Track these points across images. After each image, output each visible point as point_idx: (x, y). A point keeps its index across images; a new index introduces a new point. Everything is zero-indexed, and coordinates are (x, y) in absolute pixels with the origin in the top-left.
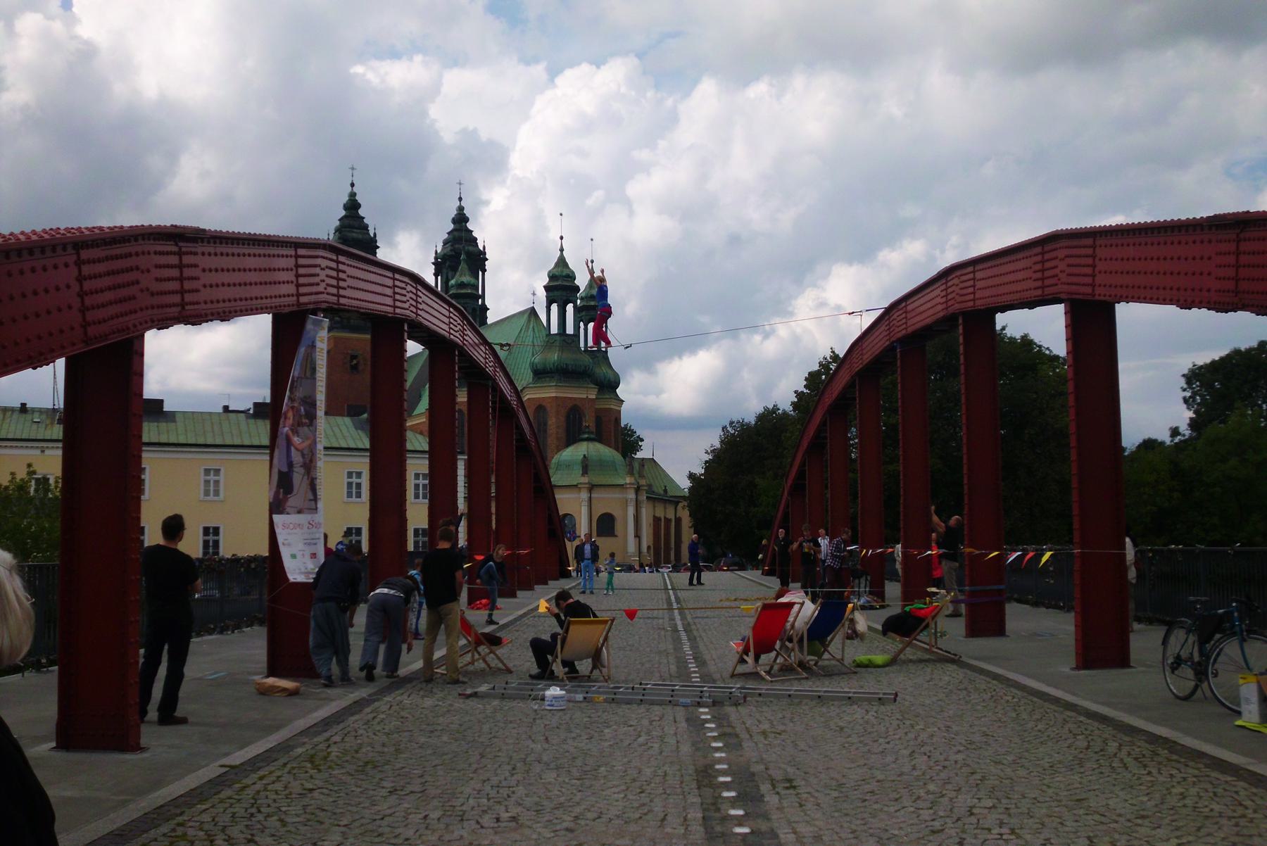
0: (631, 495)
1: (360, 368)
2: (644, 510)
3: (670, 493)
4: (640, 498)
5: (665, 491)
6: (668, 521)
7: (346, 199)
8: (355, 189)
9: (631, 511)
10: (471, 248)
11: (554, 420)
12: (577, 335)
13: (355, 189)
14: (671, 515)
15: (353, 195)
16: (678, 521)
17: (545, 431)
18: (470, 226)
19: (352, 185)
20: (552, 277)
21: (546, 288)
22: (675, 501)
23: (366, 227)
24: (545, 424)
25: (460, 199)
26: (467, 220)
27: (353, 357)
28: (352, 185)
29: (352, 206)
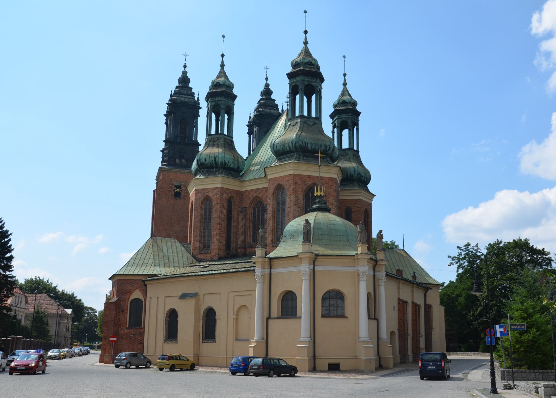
0: (365, 268)
1: (182, 195)
2: (382, 290)
3: (419, 280)
4: (377, 274)
5: (414, 277)
6: (416, 306)
7: (180, 75)
8: (186, 69)
9: (364, 288)
10: (272, 111)
11: (291, 197)
12: (318, 118)
13: (186, 69)
14: (419, 299)
15: (185, 73)
16: (428, 308)
17: (283, 210)
18: (273, 97)
19: (185, 66)
20: (295, 65)
21: (290, 76)
22: (427, 287)
23: (193, 94)
24: (284, 203)
25: (267, 79)
26: (272, 93)
27: (179, 187)
28: (185, 66)
29: (184, 80)
